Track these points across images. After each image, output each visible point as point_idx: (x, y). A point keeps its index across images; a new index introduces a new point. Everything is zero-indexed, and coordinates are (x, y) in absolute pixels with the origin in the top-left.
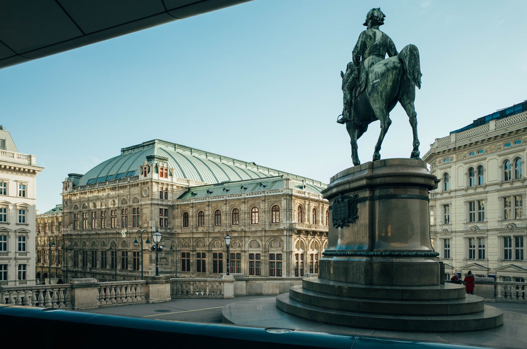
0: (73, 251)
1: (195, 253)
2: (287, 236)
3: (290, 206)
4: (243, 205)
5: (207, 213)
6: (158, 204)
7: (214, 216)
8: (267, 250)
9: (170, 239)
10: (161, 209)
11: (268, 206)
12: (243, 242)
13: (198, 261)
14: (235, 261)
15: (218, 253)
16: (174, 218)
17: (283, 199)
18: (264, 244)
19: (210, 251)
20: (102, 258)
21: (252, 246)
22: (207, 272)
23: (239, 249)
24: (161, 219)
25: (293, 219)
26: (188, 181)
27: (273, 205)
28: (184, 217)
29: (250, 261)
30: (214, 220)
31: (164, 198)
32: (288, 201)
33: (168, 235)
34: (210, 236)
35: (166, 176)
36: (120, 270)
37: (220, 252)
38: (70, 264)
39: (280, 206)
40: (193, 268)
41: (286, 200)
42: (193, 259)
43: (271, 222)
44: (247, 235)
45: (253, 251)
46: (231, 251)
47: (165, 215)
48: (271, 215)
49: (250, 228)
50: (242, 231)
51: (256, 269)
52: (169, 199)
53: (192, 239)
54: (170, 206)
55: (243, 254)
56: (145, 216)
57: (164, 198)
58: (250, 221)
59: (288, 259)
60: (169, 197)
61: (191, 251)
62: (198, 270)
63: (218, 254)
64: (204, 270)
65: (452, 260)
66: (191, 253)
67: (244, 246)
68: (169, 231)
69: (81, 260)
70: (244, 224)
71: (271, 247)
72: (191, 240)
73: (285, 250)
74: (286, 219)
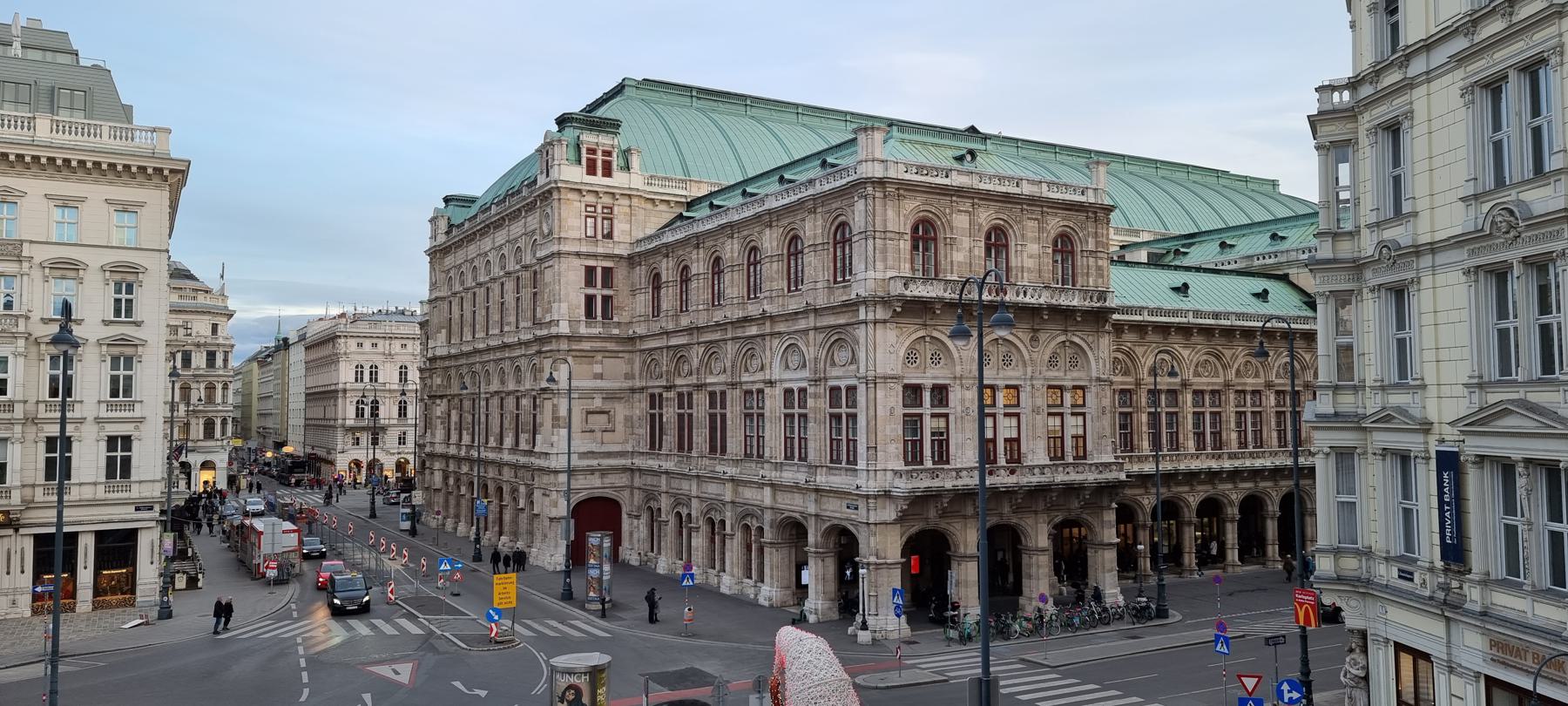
0: (445, 400)
1: (672, 394)
2: (866, 323)
3: (878, 220)
4: (767, 231)
5: (694, 271)
6: (578, 254)
7: (710, 276)
8: (822, 375)
9: (620, 355)
10: (590, 271)
11: (824, 227)
12: (768, 353)
13: (681, 416)
14: (752, 415)
15: (718, 389)
16: (633, 292)
17: (856, 198)
18: (812, 356)
19: (702, 386)
21: (790, 365)
22: (694, 454)
23: (759, 376)
24: (590, 300)
25: (890, 263)
26: (683, 181)
27: (836, 223)
28: (653, 289)
29: (786, 416)
30: (710, 291)
31: (599, 237)
32: (870, 201)
33: (613, 344)
34: (701, 340)
35: (608, 172)
36: (515, 449)
37: (723, 388)
39: (851, 223)
40: (670, 440)
41: (863, 200)
42: (670, 413)
43: (832, 279)
44: (781, 327)
45: (791, 380)
46: (747, 382)
47: (605, 285)
48: (831, 256)
49: (783, 305)
50: (765, 317)
51: (800, 438)
52: (616, 239)
53: (665, 350)
54: (620, 257)
55: (767, 390)
57: (599, 237)
58: (786, 282)
59: (872, 404)
60: (616, 233)
61: (665, 387)
62: (681, 448)
63: (718, 395)
64: (690, 449)
65: (1424, 387)
66: (665, 395)
67: (768, 365)
68: (616, 331)
69: (456, 423)
70: (767, 294)
71: (833, 364)
72: (665, 355)
73: (862, 370)
74: (863, 267)
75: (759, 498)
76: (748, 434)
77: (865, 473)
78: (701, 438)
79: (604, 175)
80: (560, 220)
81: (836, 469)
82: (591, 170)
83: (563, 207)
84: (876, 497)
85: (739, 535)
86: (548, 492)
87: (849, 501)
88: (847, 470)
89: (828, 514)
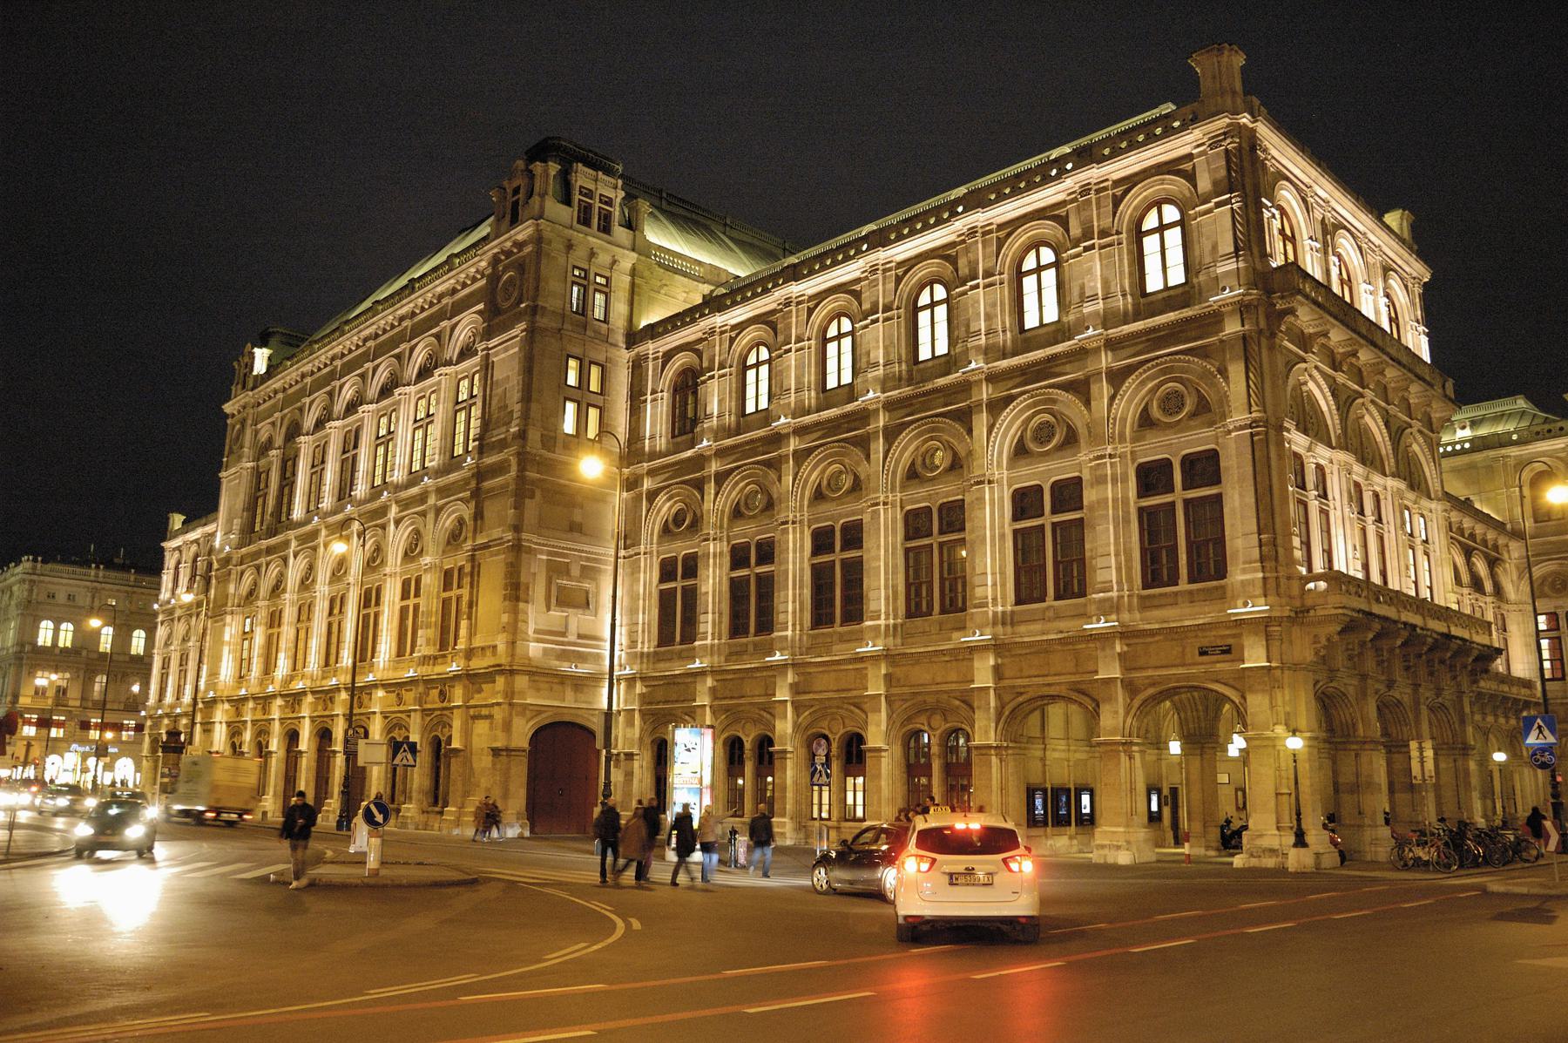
20: (330, 625)
29: (1015, 532)
38: (227, 670)
51: (1056, 563)
56: (500, 390)
62: (737, 627)
75: (953, 676)
76: (911, 581)
77: (1260, 584)
78: (793, 602)
79: (599, 229)
80: (538, 279)
81: (1165, 595)
82: (585, 220)
83: (544, 261)
84: (1279, 621)
85: (897, 750)
86: (485, 712)
87: (1205, 642)
88: (1191, 592)
89: (1150, 673)
